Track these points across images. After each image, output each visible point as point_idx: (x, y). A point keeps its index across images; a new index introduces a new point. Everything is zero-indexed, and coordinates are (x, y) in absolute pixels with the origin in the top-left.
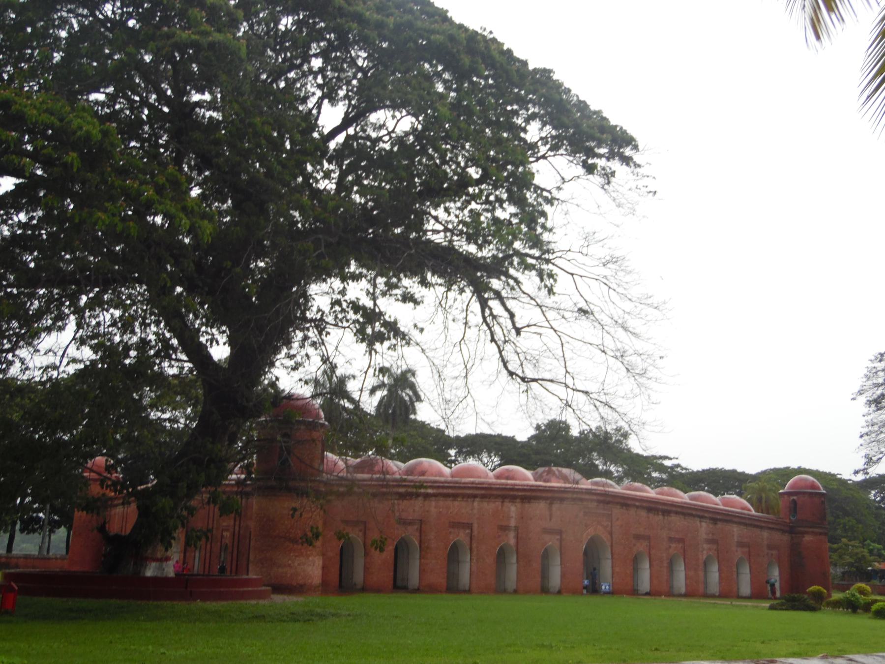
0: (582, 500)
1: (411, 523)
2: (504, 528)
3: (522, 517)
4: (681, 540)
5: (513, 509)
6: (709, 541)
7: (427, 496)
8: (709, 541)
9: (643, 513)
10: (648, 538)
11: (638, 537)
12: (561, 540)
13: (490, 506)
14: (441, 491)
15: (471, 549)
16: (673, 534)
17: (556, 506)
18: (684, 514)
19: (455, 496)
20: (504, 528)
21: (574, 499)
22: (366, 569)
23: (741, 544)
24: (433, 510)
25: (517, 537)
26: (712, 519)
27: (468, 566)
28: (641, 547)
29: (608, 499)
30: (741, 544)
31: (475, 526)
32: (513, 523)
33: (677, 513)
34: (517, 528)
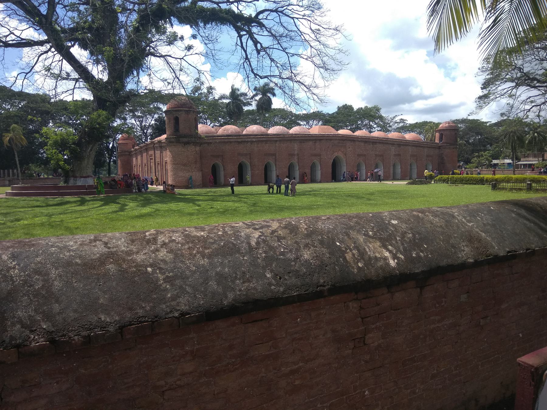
2: (292, 155)
5: (296, 146)
7: (252, 142)
9: (363, 144)
10: (365, 155)
11: (359, 155)
14: (259, 139)
15: (276, 165)
18: (383, 143)
19: (266, 142)
20: (292, 155)
21: (326, 139)
25: (298, 159)
27: (275, 172)
29: (345, 138)
32: (296, 153)
33: (380, 143)
34: (298, 155)
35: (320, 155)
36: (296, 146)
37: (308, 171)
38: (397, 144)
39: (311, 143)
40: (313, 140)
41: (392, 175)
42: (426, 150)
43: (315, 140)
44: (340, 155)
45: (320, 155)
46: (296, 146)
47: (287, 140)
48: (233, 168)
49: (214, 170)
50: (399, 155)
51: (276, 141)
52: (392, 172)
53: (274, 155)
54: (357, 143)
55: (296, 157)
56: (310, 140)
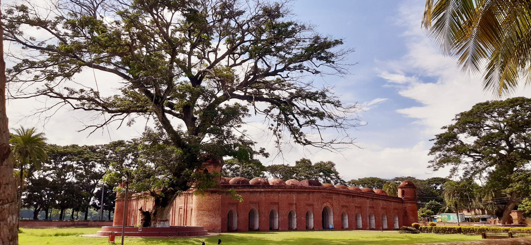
0: (321, 192)
1: (255, 203)
2: (291, 204)
3: (297, 200)
4: (360, 207)
5: (294, 197)
6: (370, 207)
8: (370, 207)
9: (345, 197)
10: (347, 207)
11: (343, 206)
12: (313, 208)
13: (285, 196)
15: (278, 213)
16: (356, 205)
17: (311, 195)
20: (291, 204)
22: (238, 222)
23: (383, 208)
24: (264, 198)
25: (296, 208)
26: (372, 198)
27: (277, 219)
28: (344, 210)
30: (383, 208)
31: (280, 203)
33: (358, 196)
34: (296, 204)
35: (312, 205)
36: (294, 196)
37: (303, 218)
38: (372, 198)
40: (307, 192)
41: (368, 224)
42: (393, 203)
43: (310, 192)
44: (328, 204)
45: (312, 205)
46: (294, 196)
47: (288, 191)
48: (244, 215)
49: (230, 216)
50: (373, 207)
51: (279, 192)
52: (368, 222)
53: (278, 203)
54: (341, 196)
55: (294, 206)
56: (305, 192)
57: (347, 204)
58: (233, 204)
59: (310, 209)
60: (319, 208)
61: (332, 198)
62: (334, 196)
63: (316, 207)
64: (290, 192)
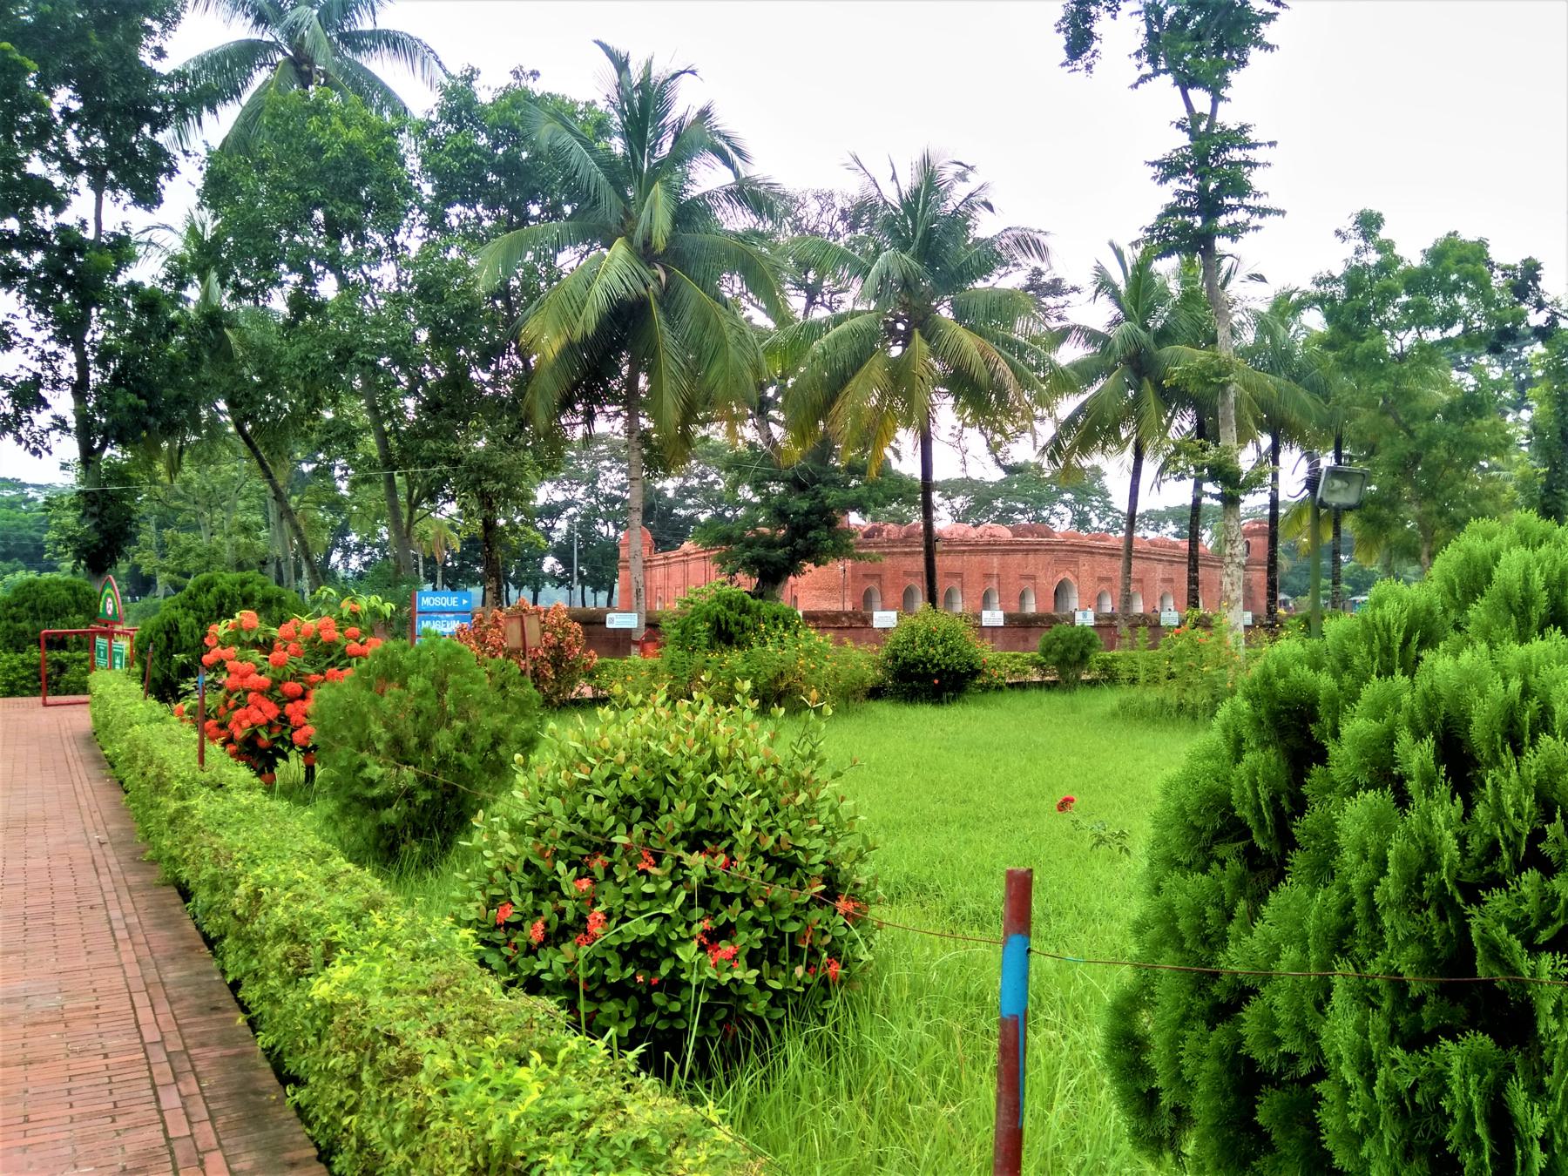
2: (988, 576)
3: (1002, 567)
5: (995, 560)
6: (1164, 580)
11: (1101, 579)
13: (975, 559)
20: (988, 576)
28: (1104, 586)
35: (1034, 578)
39: (1019, 556)
43: (1028, 551)
44: (1069, 576)
45: (1034, 578)
50: (1170, 580)
53: (960, 575)
54: (1097, 557)
55: (995, 581)
57: (1111, 575)
58: (873, 577)
59: (1027, 584)
60: (1048, 584)
61: (1076, 563)
62: (1083, 558)
63: (1041, 580)
64: (988, 551)
